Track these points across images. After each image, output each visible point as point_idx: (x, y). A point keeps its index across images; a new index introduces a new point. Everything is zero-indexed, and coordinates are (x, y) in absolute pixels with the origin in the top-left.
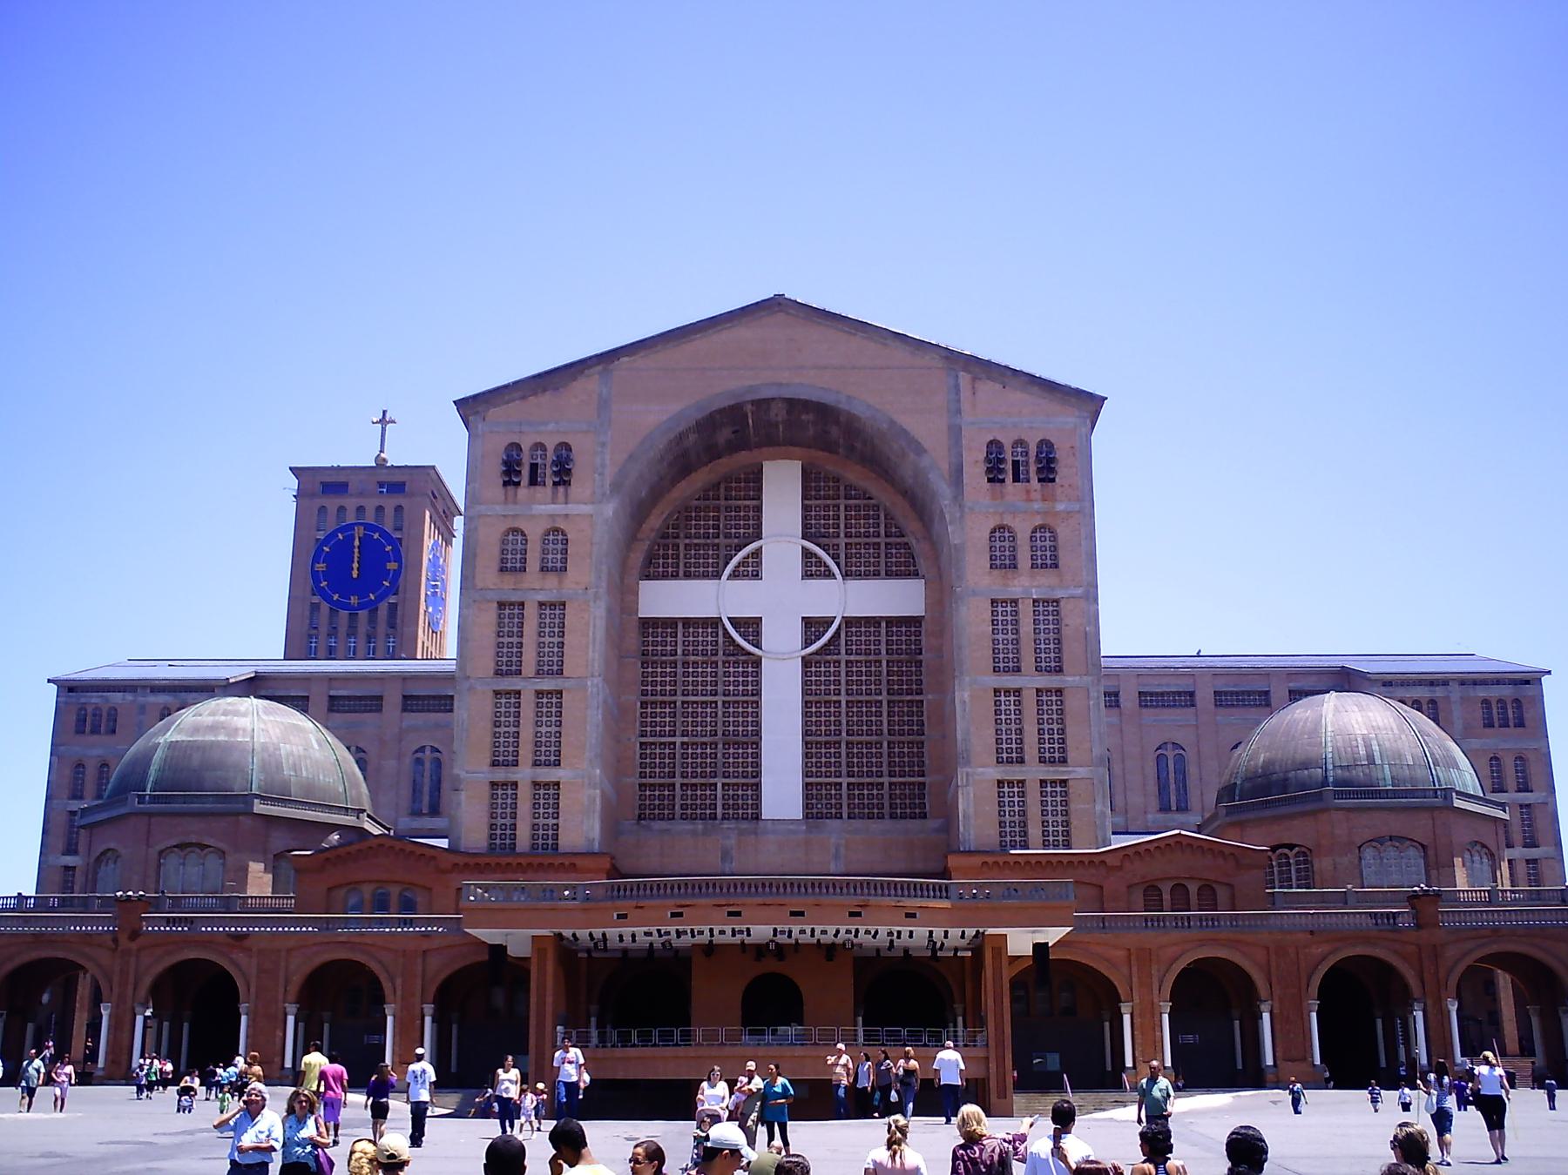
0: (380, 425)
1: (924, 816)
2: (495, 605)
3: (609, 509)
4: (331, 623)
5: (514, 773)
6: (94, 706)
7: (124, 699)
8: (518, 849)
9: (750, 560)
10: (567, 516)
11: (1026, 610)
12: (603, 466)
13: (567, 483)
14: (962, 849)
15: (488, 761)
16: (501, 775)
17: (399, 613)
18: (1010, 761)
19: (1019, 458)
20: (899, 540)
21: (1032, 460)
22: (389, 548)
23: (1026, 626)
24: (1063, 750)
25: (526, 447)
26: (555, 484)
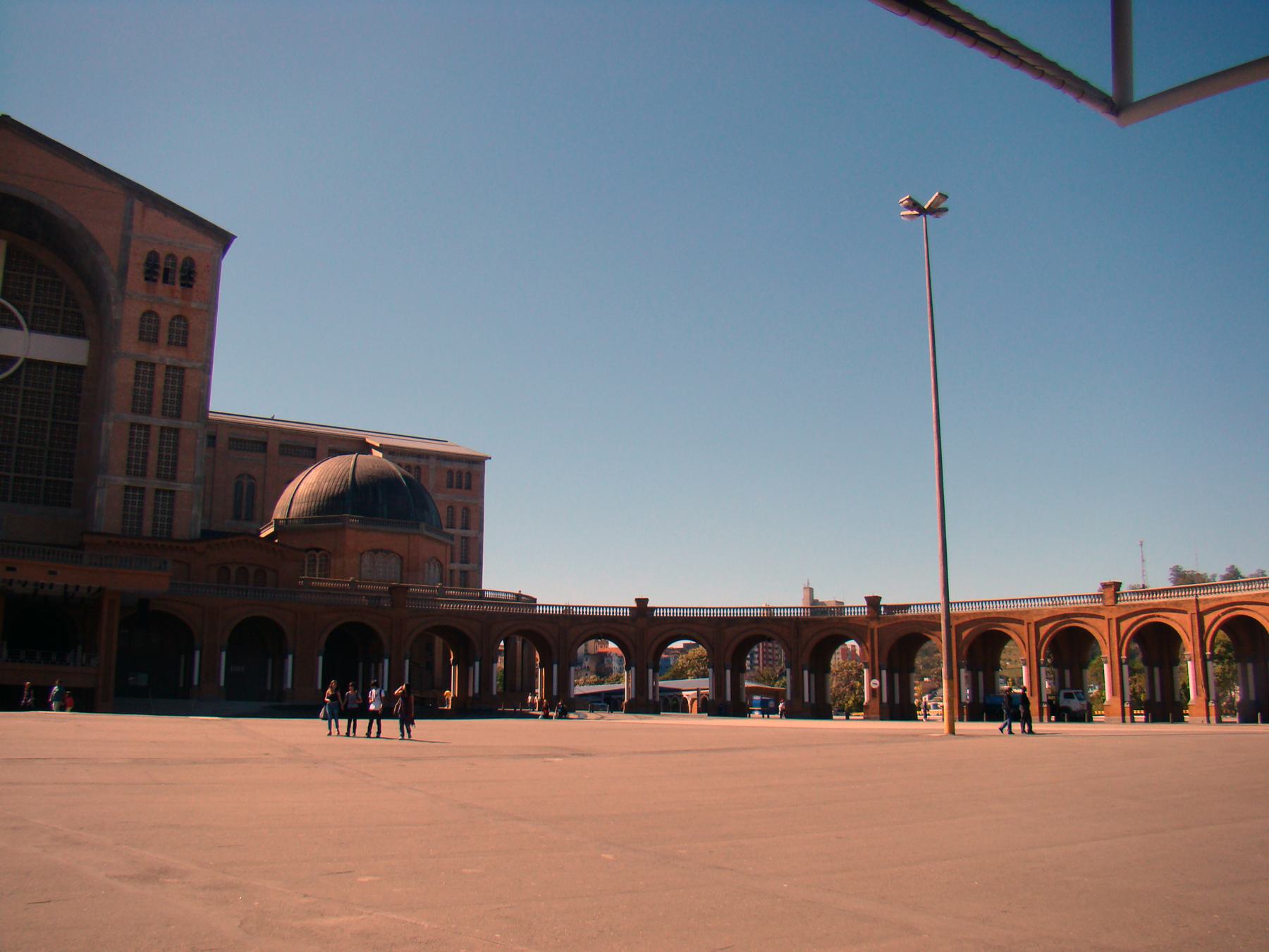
11: (160, 371)
14: (94, 530)
18: (136, 474)
19: (170, 267)
23: (159, 382)
24: (175, 470)
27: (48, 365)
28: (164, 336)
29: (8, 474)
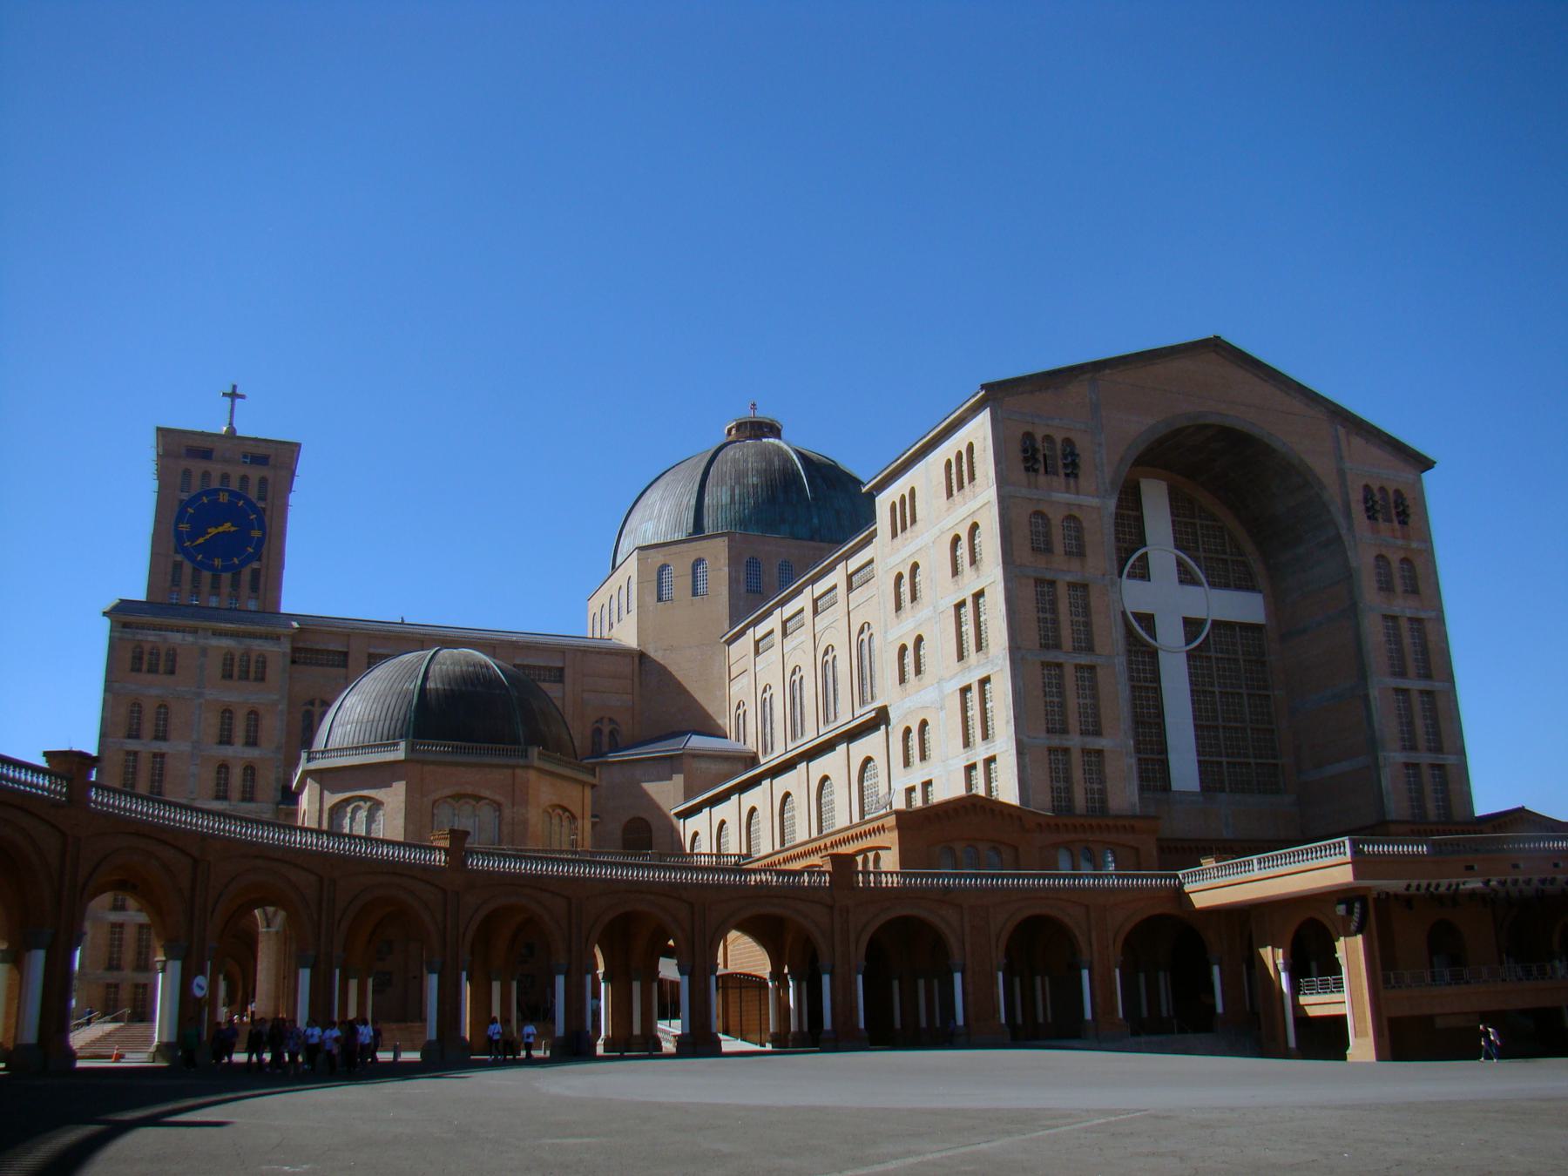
0: (228, 400)
2: (1032, 582)
3: (1112, 504)
8: (1078, 812)
9: (1136, 563)
10: (1080, 506)
13: (1076, 476)
15: (1044, 727)
16: (1056, 741)
17: (262, 579)
20: (1240, 558)
21: (1392, 505)
25: (1039, 436)
26: (1067, 475)
29: (1219, 759)
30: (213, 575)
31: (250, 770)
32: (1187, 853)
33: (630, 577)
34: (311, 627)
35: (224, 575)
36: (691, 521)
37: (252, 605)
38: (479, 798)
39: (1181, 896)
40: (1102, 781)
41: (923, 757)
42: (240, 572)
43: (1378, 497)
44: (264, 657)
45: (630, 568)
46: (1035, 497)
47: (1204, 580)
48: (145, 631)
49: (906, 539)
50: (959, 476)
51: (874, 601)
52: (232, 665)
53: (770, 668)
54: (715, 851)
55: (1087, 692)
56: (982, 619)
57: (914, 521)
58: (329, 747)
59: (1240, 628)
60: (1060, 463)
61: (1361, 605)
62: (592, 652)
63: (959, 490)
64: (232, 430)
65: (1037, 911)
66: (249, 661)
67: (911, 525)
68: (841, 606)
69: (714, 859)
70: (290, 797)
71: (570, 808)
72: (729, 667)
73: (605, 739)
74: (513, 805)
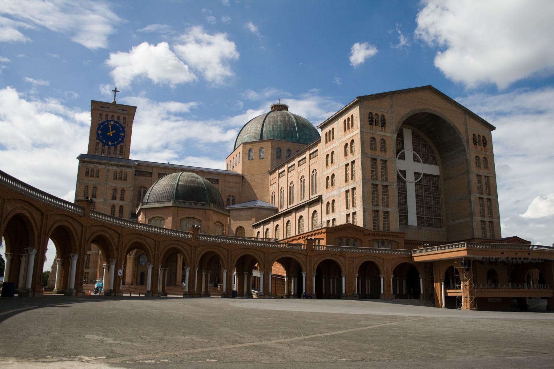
0: (114, 92)
1: (441, 227)
2: (370, 159)
3: (395, 136)
4: (102, 149)
5: (378, 208)
6: (92, 168)
7: (102, 167)
10: (385, 136)
12: (393, 123)
13: (385, 127)
17: (124, 149)
20: (433, 155)
21: (482, 140)
22: (121, 129)
25: (374, 114)
26: (382, 126)
27: (428, 175)
28: (482, 165)
29: (424, 216)
30: (108, 147)
31: (121, 208)
32: (415, 244)
33: (240, 152)
34: (141, 164)
35: (112, 147)
36: (260, 135)
37: (121, 157)
38: (194, 218)
39: (411, 258)
40: (388, 221)
41: (333, 211)
42: (117, 146)
43: (477, 138)
44: (127, 173)
45: (241, 149)
46: (372, 133)
47: (421, 161)
48: (89, 164)
49: (330, 144)
50: (348, 125)
51: (318, 163)
52: (117, 175)
53: (283, 182)
54: (265, 237)
55: (385, 193)
56: (354, 169)
57: (333, 138)
58: (148, 202)
59: (432, 176)
60: (380, 123)
61: (470, 171)
62: (228, 175)
63: (348, 129)
64: (115, 102)
65: (369, 260)
66: (122, 174)
67: (332, 139)
68: (307, 164)
69: (264, 240)
70: (135, 216)
71: (222, 223)
72: (270, 181)
73: (231, 201)
74: (205, 221)
